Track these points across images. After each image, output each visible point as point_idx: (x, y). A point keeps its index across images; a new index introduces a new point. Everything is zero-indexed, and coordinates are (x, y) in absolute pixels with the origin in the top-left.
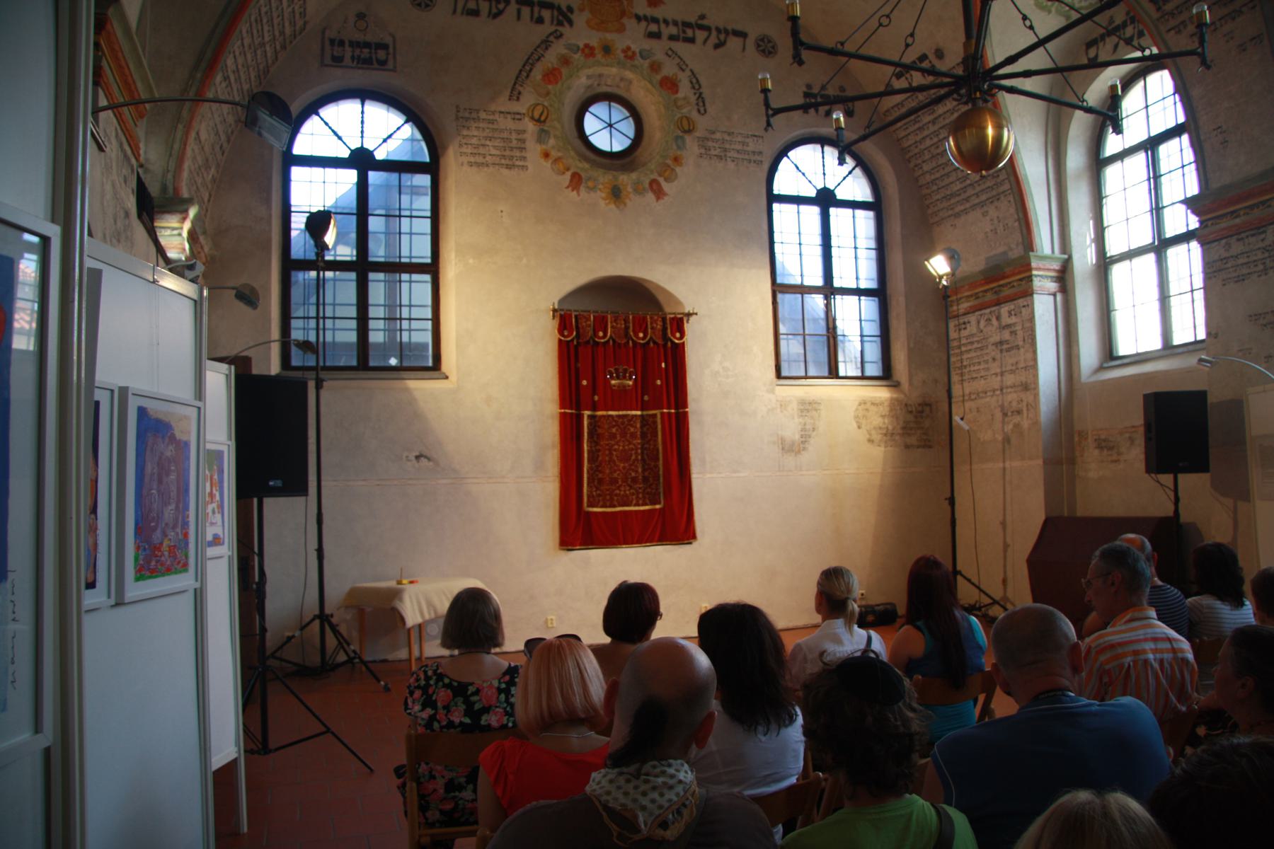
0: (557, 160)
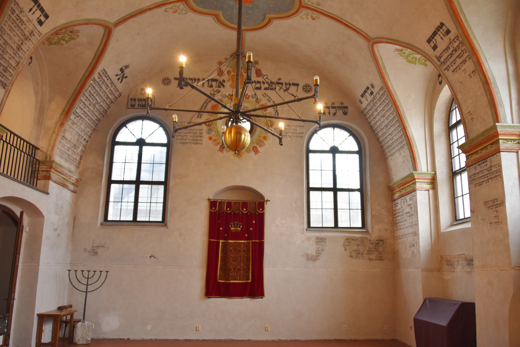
0: (215, 140)
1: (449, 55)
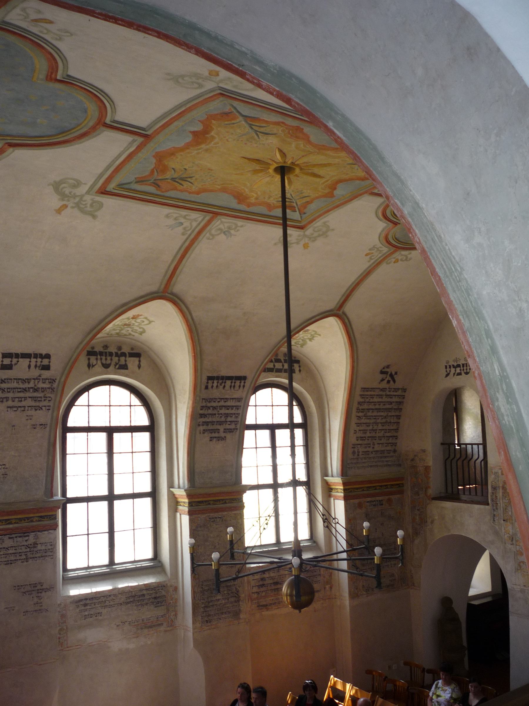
1: (20, 388)
